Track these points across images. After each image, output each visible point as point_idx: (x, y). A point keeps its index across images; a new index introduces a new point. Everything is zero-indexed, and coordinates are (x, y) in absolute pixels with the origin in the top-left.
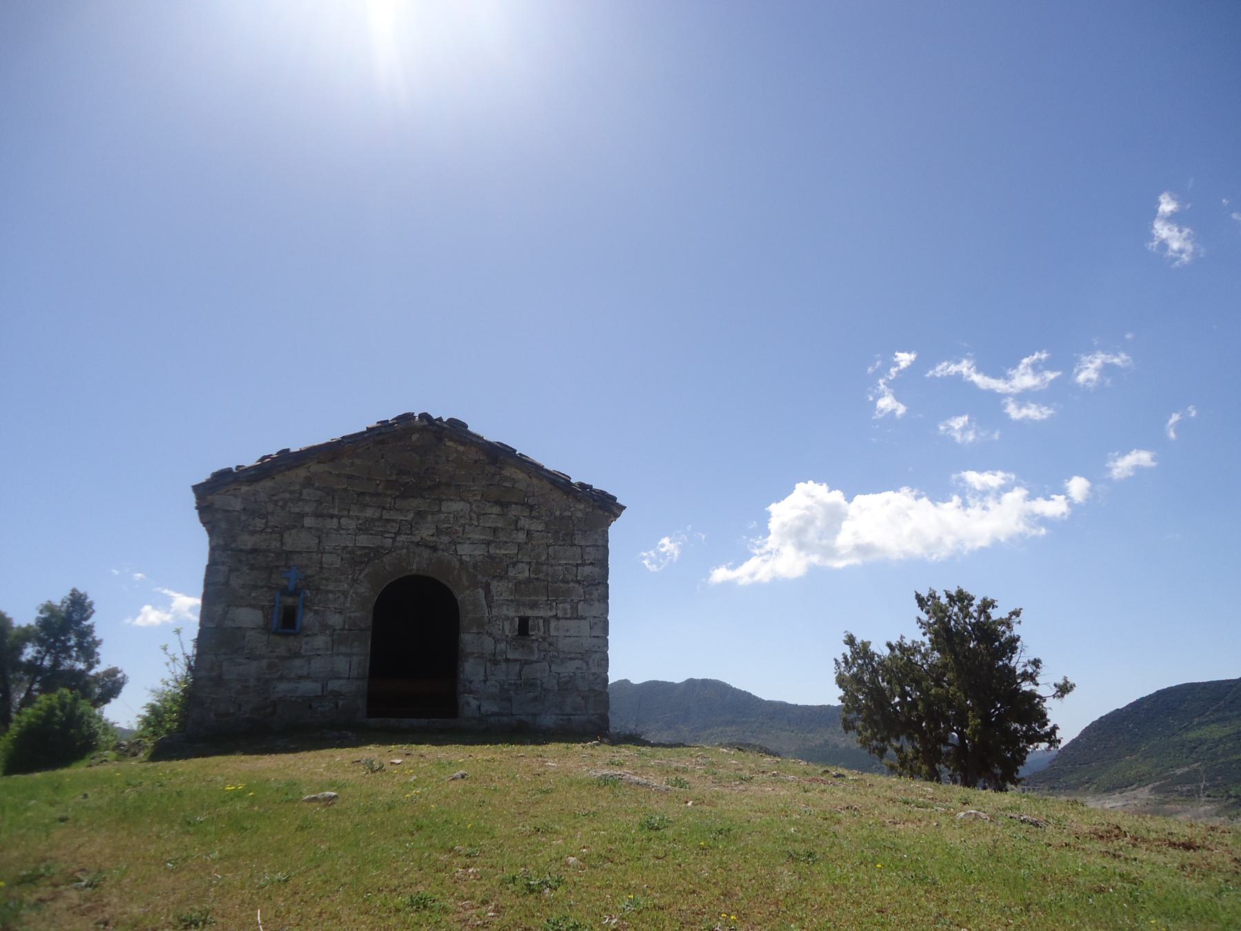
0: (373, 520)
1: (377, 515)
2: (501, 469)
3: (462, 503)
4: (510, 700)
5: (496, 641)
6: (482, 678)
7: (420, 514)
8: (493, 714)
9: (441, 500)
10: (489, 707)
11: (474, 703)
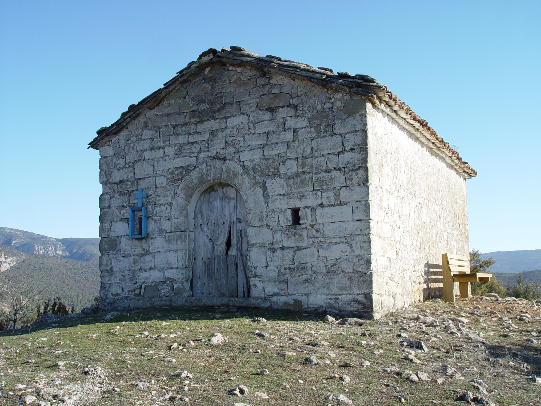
0: (184, 145)
1: (186, 141)
2: (269, 79)
3: (242, 117)
4: (286, 282)
5: (274, 232)
6: (265, 265)
7: (213, 133)
8: (276, 294)
9: (226, 118)
10: (271, 289)
11: (260, 285)
